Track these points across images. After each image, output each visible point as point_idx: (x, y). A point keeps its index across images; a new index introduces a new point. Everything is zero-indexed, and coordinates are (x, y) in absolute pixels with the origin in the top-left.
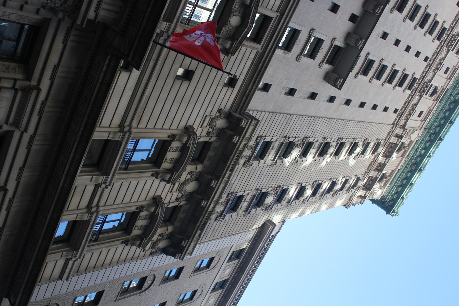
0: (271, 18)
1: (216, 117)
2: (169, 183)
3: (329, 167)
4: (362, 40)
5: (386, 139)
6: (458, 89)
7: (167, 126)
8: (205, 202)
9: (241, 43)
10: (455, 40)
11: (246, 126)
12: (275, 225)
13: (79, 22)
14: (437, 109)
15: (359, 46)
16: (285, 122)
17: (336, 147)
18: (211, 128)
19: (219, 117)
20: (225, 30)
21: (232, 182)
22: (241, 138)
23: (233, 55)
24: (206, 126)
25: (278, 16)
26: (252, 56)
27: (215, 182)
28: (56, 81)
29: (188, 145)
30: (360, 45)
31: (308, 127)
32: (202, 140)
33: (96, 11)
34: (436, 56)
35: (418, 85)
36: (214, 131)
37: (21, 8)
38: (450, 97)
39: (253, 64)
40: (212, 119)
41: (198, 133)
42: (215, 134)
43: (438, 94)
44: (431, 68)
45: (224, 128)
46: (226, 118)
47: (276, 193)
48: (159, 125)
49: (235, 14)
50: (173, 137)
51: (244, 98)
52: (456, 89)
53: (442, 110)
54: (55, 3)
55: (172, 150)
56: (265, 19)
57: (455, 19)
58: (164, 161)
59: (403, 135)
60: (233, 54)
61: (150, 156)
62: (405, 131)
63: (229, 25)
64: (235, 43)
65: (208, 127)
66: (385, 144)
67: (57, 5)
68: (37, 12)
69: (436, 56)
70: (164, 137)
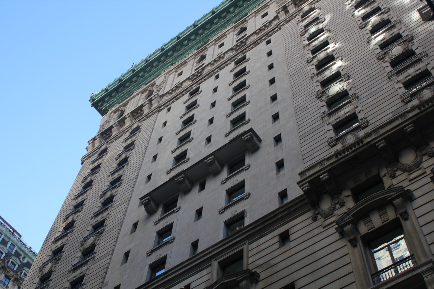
2: (408, 190)
3: (341, 34)
4: (206, 162)
5: (295, 16)
6: (227, 18)
8: (407, 130)
10: (198, 72)
11: (306, 183)
12: (419, 11)
14: (253, 9)
15: (212, 159)
16: (308, 137)
17: (316, 56)
21: (391, 115)
22: (318, 174)
25: (214, 260)
26: (254, 245)
27: (379, 145)
30: (210, 159)
31: (306, 108)
34: (211, 73)
35: (238, 56)
38: (238, 14)
39: (261, 236)
43: (241, 26)
44: (220, 64)
47: (387, 54)
51: (293, 209)
52: (229, 19)
53: (251, 5)
57: (180, 97)
58: (389, 221)
59: (282, 9)
62: (278, 12)
64: (239, 279)
66: (299, 12)
69: (211, 73)
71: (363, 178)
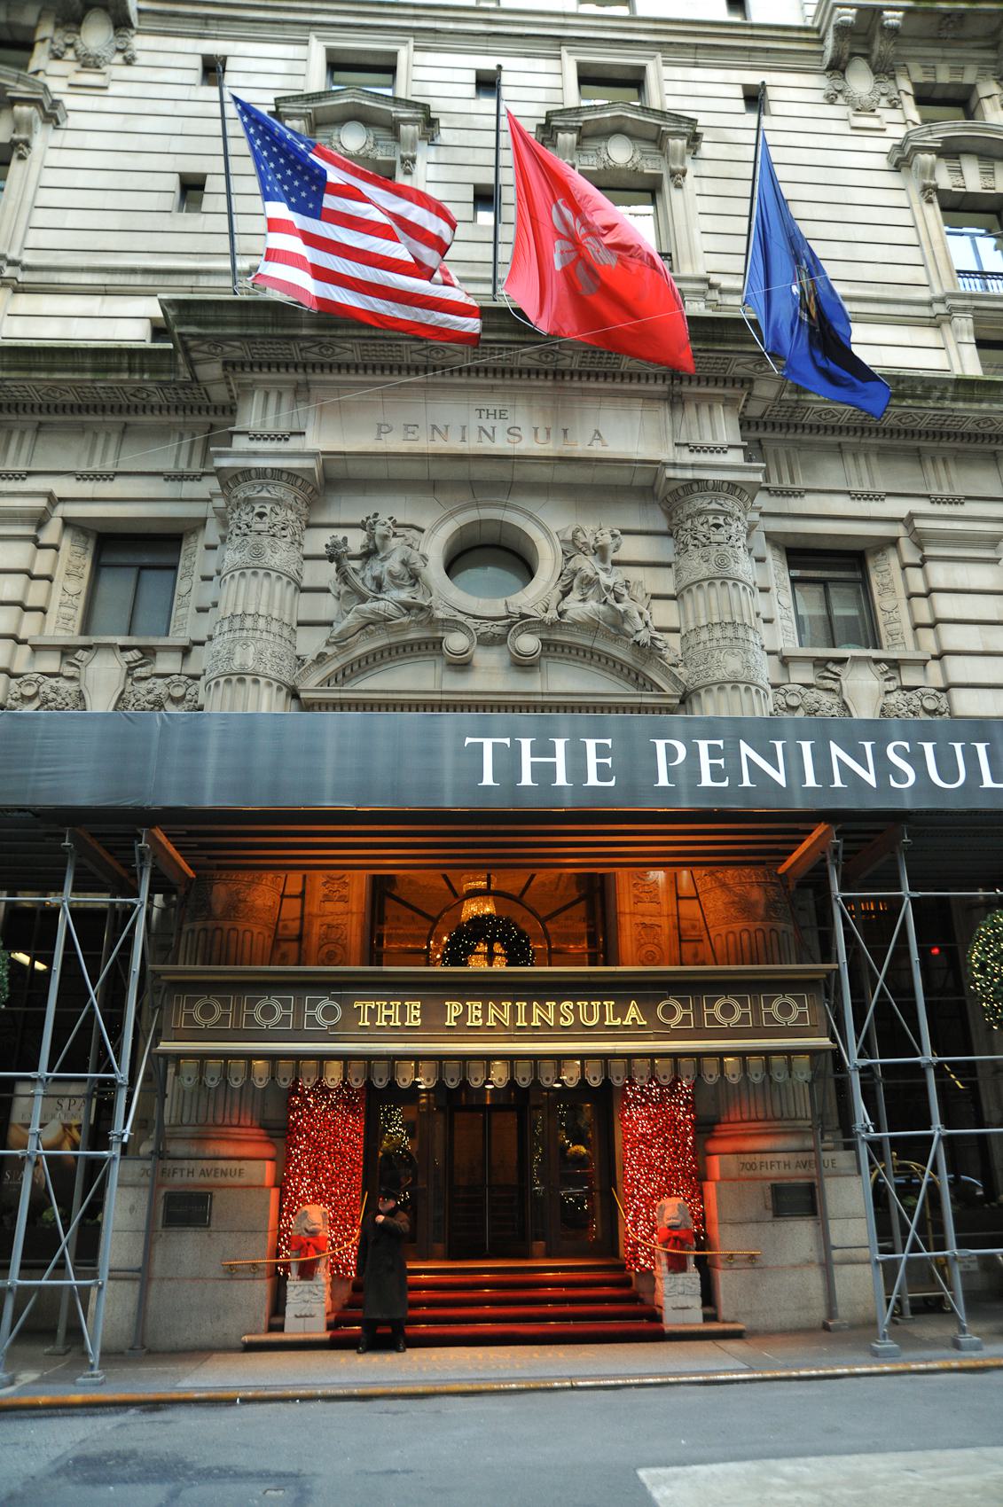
0: (580, 66)
1: (850, 102)
7: (904, 217)
9: (663, 114)
13: (759, 477)
18: (878, 102)
19: (846, 94)
20: (649, 168)
23: (696, 120)
24: (878, 117)
26: (678, 72)
28: (882, 488)
29: (939, 145)
32: (913, 113)
33: (722, 450)
36: (884, 91)
37: (764, 590)
40: (858, 110)
41: (900, 132)
42: (891, 84)
45: (870, 66)
46: (843, 71)
48: (908, 236)
49: (606, 157)
50: (930, 192)
54: (738, 531)
55: (960, 183)
56: (589, 78)
58: (993, 192)
60: (693, 121)
61: (983, 231)
63: (635, 160)
65: (878, 112)
67: (741, 528)
68: (760, 560)
70: (933, 213)
71: (944, 76)
